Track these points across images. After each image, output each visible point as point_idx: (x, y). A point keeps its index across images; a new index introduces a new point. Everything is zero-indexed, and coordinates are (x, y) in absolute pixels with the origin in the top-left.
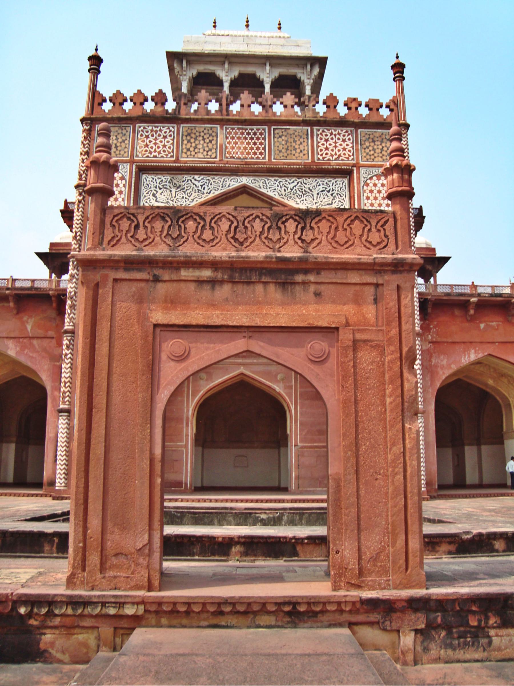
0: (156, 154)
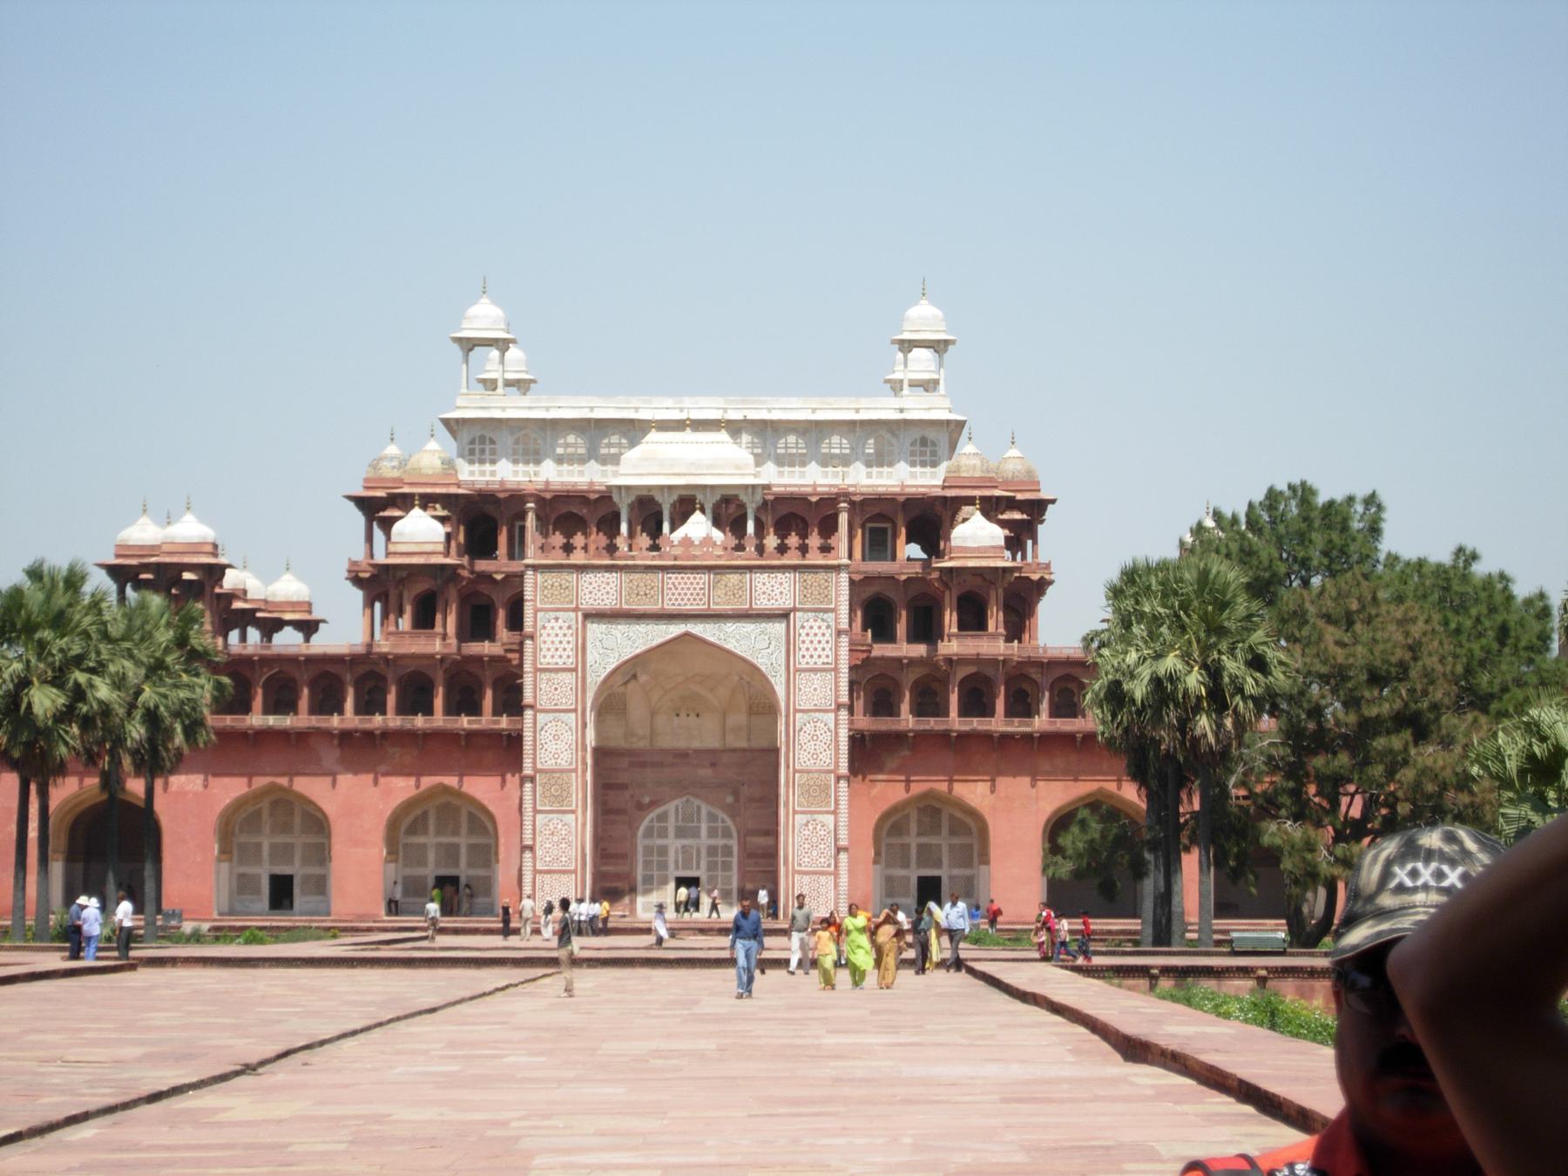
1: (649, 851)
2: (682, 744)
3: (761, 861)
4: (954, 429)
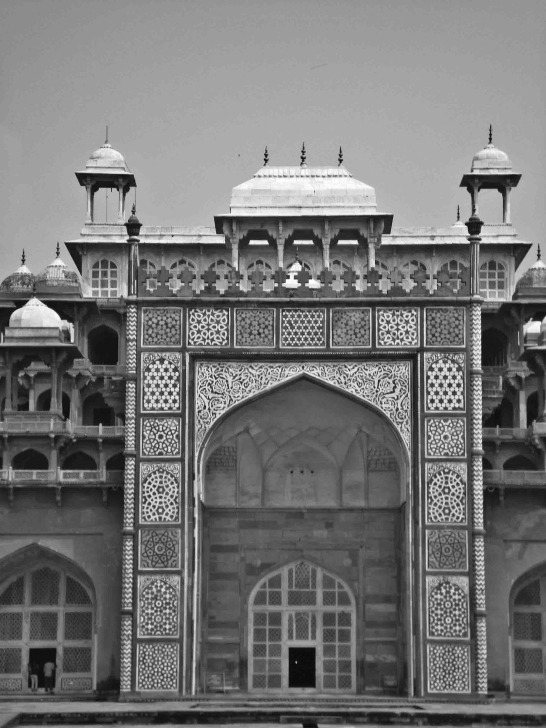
0: (209, 341)
1: (260, 618)
2: (297, 504)
3: (382, 630)
4: (519, 251)
